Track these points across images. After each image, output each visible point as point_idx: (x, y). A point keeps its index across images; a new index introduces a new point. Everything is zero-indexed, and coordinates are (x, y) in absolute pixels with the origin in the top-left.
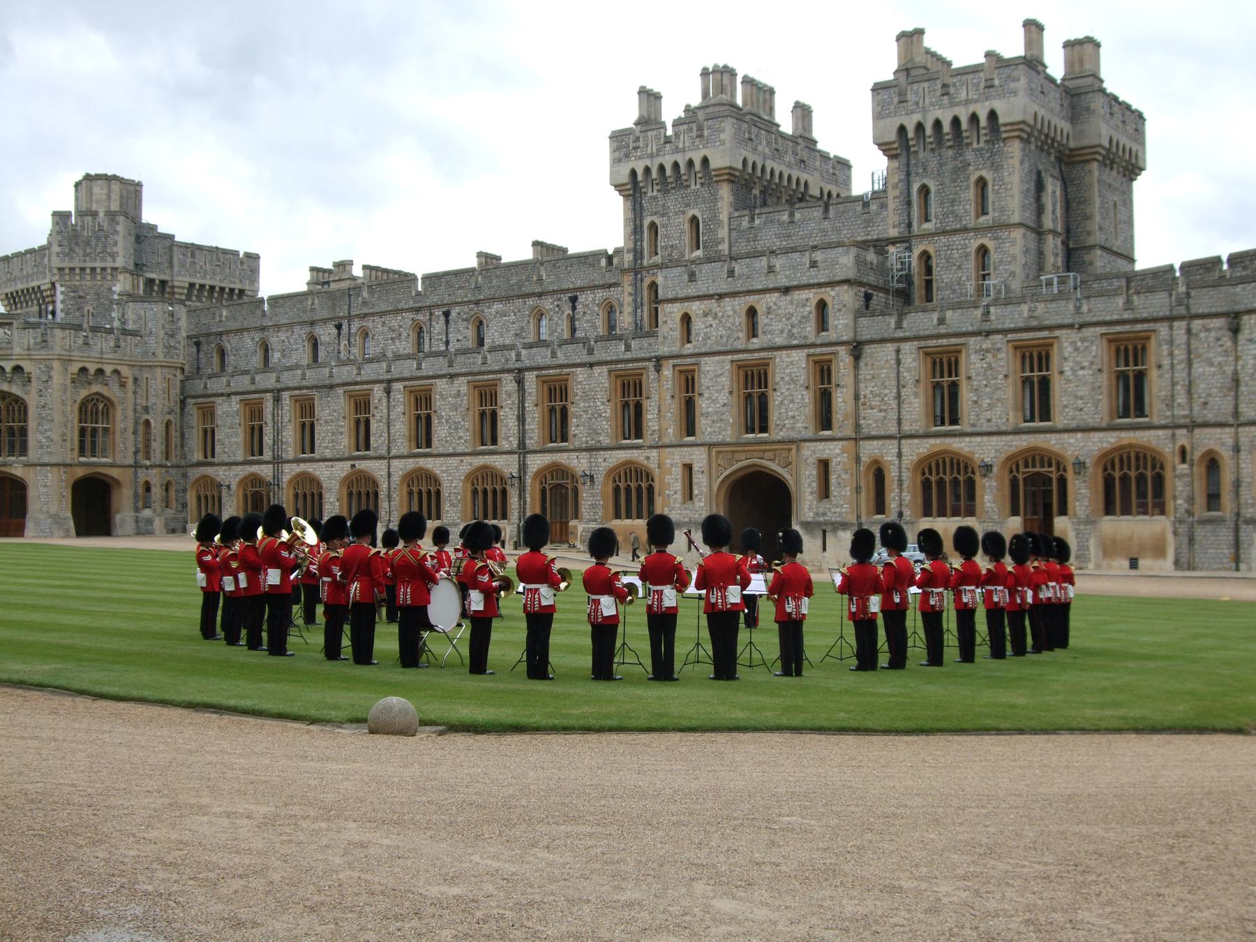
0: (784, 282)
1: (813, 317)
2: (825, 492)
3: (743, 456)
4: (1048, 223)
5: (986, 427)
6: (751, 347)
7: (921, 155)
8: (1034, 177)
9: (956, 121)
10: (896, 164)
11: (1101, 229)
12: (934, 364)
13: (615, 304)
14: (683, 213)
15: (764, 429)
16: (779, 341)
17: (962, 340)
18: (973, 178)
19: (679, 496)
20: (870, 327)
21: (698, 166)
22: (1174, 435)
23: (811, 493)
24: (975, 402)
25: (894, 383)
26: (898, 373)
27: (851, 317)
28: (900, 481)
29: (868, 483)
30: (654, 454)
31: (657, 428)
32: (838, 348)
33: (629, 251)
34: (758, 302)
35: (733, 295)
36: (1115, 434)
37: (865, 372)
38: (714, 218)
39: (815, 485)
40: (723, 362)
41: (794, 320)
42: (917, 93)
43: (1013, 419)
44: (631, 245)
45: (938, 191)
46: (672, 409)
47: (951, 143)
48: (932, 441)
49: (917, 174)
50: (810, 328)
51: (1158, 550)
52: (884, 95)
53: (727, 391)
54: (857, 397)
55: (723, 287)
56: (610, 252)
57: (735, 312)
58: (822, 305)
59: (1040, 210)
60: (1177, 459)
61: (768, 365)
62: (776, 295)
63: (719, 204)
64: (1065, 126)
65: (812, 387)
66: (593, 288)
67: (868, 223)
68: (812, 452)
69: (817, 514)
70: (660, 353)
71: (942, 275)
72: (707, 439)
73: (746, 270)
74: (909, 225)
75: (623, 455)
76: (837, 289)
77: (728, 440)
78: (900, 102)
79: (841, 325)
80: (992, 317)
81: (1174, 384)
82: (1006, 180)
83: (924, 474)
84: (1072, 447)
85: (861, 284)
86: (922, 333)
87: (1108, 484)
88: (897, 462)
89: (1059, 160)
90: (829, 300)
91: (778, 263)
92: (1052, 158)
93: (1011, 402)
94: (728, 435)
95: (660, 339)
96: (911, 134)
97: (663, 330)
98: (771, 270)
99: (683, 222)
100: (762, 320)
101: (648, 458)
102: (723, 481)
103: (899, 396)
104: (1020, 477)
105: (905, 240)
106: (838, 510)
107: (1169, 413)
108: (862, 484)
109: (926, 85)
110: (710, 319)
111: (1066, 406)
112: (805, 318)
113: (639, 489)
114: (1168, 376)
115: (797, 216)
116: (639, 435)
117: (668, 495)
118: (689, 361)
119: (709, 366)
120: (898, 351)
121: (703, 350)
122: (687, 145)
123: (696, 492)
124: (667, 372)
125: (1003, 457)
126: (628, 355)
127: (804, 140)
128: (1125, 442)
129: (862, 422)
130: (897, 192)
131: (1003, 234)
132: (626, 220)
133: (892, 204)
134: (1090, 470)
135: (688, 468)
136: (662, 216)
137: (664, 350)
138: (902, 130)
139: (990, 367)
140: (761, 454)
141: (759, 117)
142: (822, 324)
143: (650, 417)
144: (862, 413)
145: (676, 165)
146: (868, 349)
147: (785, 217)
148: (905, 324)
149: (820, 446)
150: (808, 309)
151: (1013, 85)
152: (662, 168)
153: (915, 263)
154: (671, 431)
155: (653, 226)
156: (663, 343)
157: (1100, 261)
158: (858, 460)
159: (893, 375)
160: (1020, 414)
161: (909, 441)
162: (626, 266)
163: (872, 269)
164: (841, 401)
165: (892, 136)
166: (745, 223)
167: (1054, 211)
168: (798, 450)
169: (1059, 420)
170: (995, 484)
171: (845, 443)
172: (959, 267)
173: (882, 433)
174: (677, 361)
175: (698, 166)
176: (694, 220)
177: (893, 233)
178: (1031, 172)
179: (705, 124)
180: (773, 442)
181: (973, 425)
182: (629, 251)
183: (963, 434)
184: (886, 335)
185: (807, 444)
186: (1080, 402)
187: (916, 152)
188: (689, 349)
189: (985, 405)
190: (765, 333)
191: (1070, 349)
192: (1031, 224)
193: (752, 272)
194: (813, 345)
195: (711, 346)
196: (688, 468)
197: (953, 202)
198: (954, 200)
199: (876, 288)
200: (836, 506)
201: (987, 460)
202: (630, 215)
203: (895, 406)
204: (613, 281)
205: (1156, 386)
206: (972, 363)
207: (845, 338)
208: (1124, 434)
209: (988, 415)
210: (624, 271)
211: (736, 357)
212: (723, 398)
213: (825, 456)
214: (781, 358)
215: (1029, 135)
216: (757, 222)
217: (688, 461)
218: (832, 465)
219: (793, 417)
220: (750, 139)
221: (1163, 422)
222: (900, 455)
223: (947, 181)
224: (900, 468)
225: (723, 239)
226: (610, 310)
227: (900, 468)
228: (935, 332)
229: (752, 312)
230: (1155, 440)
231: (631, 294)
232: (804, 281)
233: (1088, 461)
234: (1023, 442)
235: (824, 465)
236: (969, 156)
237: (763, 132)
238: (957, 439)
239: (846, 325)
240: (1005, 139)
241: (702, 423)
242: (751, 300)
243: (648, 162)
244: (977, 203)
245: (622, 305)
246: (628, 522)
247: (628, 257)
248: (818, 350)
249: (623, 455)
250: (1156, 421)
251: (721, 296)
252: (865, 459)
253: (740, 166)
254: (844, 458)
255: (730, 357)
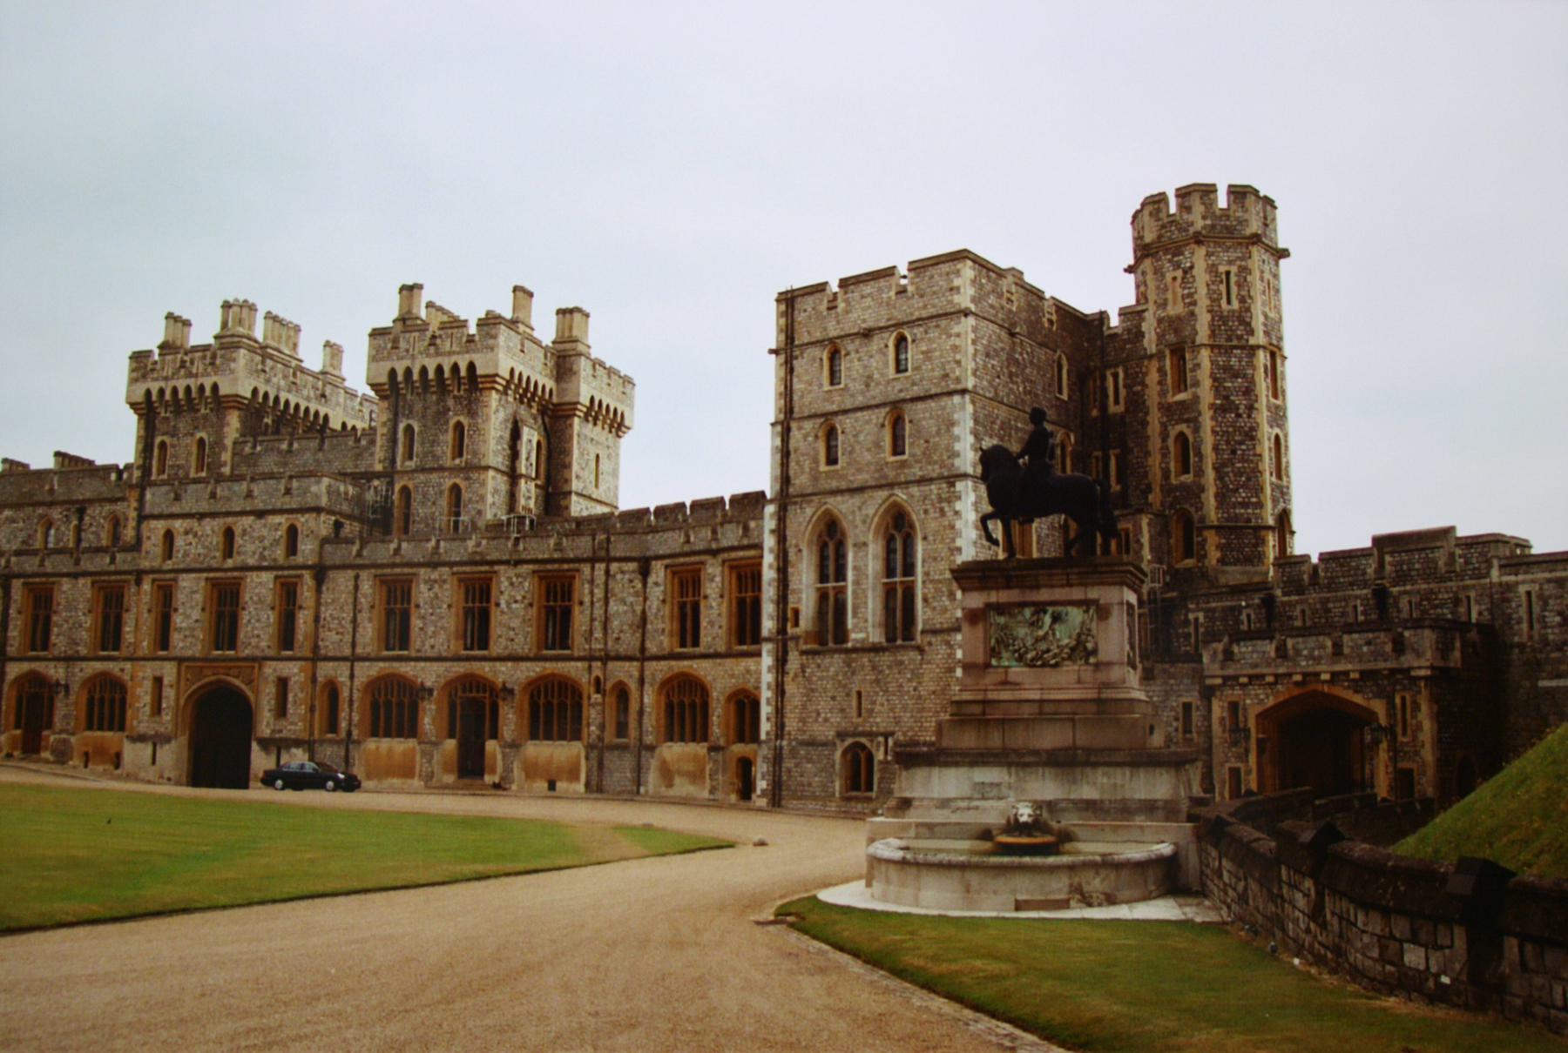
0: (261, 506)
1: (283, 542)
2: (281, 711)
3: (206, 672)
4: (522, 468)
5: (430, 653)
6: (226, 566)
7: (409, 397)
8: (510, 426)
9: (440, 369)
10: (385, 404)
11: (577, 477)
12: (389, 592)
13: (122, 518)
14: (192, 435)
15: (232, 645)
16: (251, 562)
17: (414, 570)
18: (452, 423)
19: (147, 709)
20: (336, 554)
21: (208, 392)
22: (590, 667)
23: (270, 710)
24: (421, 629)
25: (351, 607)
26: (356, 599)
27: (317, 543)
28: (351, 702)
29: (321, 703)
30: (128, 666)
31: (132, 640)
32: (304, 572)
33: (138, 468)
34: (235, 523)
35: (213, 515)
36: (541, 664)
37: (327, 597)
38: (219, 444)
39: (273, 702)
40: (199, 579)
41: (266, 543)
42: (408, 342)
43: (456, 647)
44: (141, 462)
45: (421, 432)
46: (148, 621)
47: (434, 389)
48: (381, 664)
49: (404, 415)
50: (279, 553)
51: (573, 775)
52: (380, 341)
53: (200, 607)
54: (317, 619)
55: (204, 507)
56: (121, 467)
57: (213, 532)
58: (292, 532)
59: (514, 455)
60: (592, 689)
61: (239, 584)
62: (252, 518)
63: (226, 429)
64: (551, 384)
65: (277, 608)
66: (102, 500)
67: (358, 456)
68: (271, 670)
69: (273, 731)
70: (142, 567)
71: (420, 510)
72: (176, 652)
73: (226, 493)
74: (393, 461)
75: (98, 666)
76: (307, 516)
77: (197, 655)
78: (393, 348)
79: (307, 549)
80: (442, 551)
81: (592, 620)
82: (480, 426)
83: (373, 695)
84: (502, 673)
85: (330, 512)
86: (379, 561)
87: (534, 707)
88: (349, 683)
89: (543, 411)
90: (299, 526)
91: (257, 488)
92: (534, 411)
93: (452, 629)
94: (196, 650)
95: (143, 554)
96: (400, 378)
97: (146, 545)
98: (249, 495)
99: (190, 443)
100: (238, 541)
101: (122, 670)
102: (190, 696)
103: (354, 621)
104: (458, 701)
105: (389, 475)
106: (293, 727)
107: (587, 647)
108: (317, 703)
109: (417, 334)
110: (190, 536)
111: (500, 636)
112: (277, 542)
113: (113, 700)
114: (588, 612)
115: (296, 445)
116: (117, 647)
117: (138, 709)
118: (168, 576)
119: (186, 582)
120: (357, 577)
121: (182, 566)
122: (200, 370)
123: (164, 705)
124: (146, 586)
125: (443, 681)
126: (112, 568)
127: (328, 380)
128: (548, 672)
129: (320, 643)
130: (385, 430)
131: (474, 476)
132: (139, 438)
133: (380, 441)
134: (517, 697)
135: (158, 681)
136: (173, 436)
137: (146, 564)
138: (393, 373)
139: (436, 597)
140: (222, 671)
141: (280, 352)
142: (292, 548)
143: (127, 629)
144: (322, 634)
145: (188, 389)
146: (331, 574)
147: (284, 446)
148: (365, 553)
149: (280, 665)
150: (279, 533)
151: (491, 342)
152: (175, 391)
153: (396, 497)
154: (145, 644)
155: (163, 445)
156: (145, 558)
157: (578, 508)
158: (314, 679)
159: (351, 600)
160: (461, 642)
161: (361, 664)
162: (134, 481)
163: (346, 499)
164: (303, 620)
165: (384, 379)
166: (247, 449)
167: (527, 459)
168: (260, 667)
169: (496, 648)
170: (433, 707)
171: (303, 663)
172: (434, 503)
173: (338, 654)
174: (156, 576)
175: (208, 392)
176: (201, 442)
177: (379, 467)
178: (506, 421)
179: (219, 353)
180: (238, 659)
181: (418, 651)
182: (138, 468)
183: (408, 659)
184: (348, 562)
185: (269, 663)
186: (512, 633)
187: (405, 395)
188: (169, 565)
189: (430, 633)
190: (239, 553)
191: (506, 584)
192: (504, 469)
193: (234, 495)
194: (282, 568)
195: (189, 562)
196: (158, 681)
197: (433, 443)
198: (434, 441)
199: (350, 517)
200: (292, 724)
201: (428, 684)
202: (142, 432)
203: (351, 630)
204: (119, 495)
205: (580, 620)
206: (422, 593)
207: (310, 563)
208: (548, 665)
209: (432, 641)
210: (131, 487)
211: (212, 575)
212: (196, 614)
213: (285, 673)
214: (253, 579)
215: (507, 388)
216: (259, 448)
217: (158, 674)
218: (291, 683)
219: (258, 636)
220: (264, 371)
221: (582, 654)
222: (352, 676)
223: (429, 424)
224: (351, 690)
225: (225, 464)
226: (116, 523)
227: (351, 690)
228: (391, 561)
229: (229, 534)
230: (575, 670)
231: (136, 509)
232: (278, 505)
233: (516, 688)
234: (460, 668)
235: (283, 683)
236: (450, 402)
237: (279, 366)
238: (403, 664)
239: (312, 550)
240: (481, 390)
241: (175, 638)
242: (230, 520)
243: (162, 384)
244: (453, 446)
245: (127, 519)
246: (99, 733)
247: (137, 473)
248: (286, 573)
249: (98, 666)
250: (576, 653)
251: (201, 516)
252: (320, 679)
253: (249, 395)
254: (302, 677)
255: (205, 575)
